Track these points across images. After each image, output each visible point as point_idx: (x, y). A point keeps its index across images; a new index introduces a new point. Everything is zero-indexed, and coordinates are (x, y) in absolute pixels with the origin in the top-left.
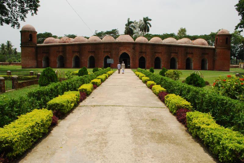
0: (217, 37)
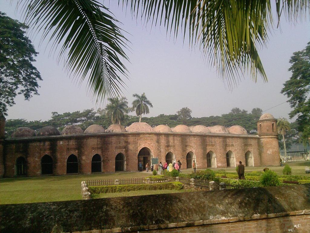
0: (260, 123)
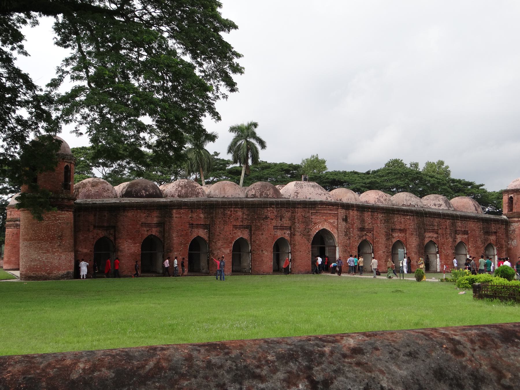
0: (512, 195)
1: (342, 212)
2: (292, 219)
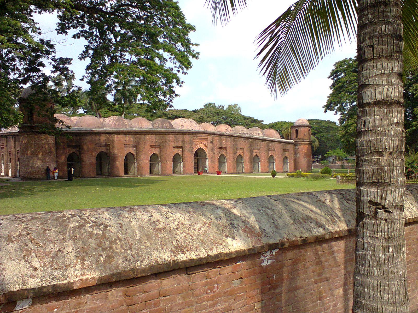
0: (297, 128)
1: (210, 137)
2: (183, 141)
